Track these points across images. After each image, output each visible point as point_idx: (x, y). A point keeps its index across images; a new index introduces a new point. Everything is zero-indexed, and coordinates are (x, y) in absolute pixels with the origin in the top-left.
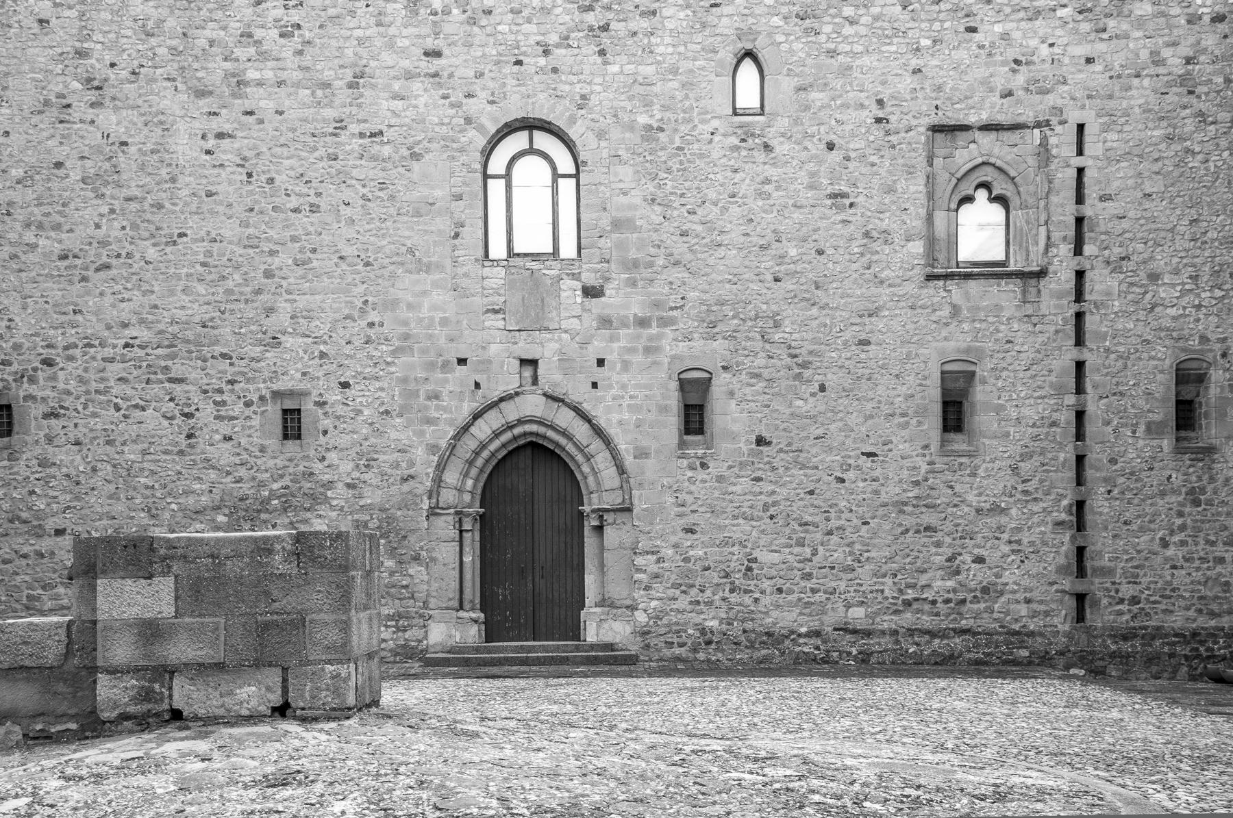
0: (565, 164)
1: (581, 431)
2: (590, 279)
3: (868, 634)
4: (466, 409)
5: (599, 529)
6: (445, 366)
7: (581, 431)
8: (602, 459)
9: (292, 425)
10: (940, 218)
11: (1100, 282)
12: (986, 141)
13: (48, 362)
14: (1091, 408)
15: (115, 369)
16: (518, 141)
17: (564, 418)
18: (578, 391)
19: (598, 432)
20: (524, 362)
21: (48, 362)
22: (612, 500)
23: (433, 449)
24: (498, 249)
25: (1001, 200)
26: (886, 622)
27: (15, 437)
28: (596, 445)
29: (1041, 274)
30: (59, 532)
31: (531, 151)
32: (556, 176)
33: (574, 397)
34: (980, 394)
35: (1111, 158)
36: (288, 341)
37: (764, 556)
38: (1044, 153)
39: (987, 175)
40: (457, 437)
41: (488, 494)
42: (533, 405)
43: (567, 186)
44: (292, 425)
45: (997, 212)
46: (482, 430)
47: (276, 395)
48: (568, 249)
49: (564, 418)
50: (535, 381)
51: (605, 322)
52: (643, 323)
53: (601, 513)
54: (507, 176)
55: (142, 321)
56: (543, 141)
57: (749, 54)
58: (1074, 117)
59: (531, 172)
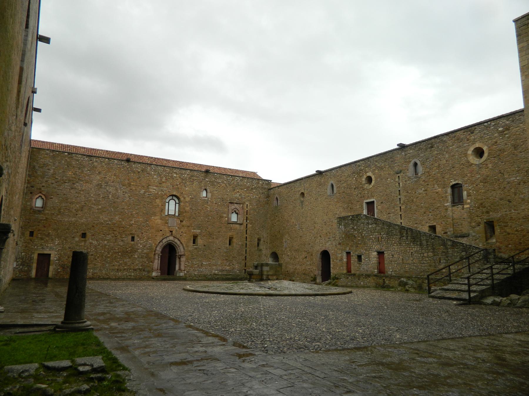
0: (177, 202)
1: (178, 243)
2: (181, 219)
3: (218, 275)
4: (161, 238)
5: (180, 258)
6: (158, 231)
7: (178, 243)
8: (181, 247)
9: (133, 239)
10: (230, 215)
11: (249, 226)
12: (236, 205)
13: (93, 226)
14: (248, 243)
15: (105, 228)
16: (171, 198)
17: (176, 240)
18: (178, 236)
19: (181, 243)
20: (171, 231)
21: (93, 226)
22: (183, 253)
23: (155, 244)
24: (166, 214)
25: (237, 213)
26: (220, 273)
27: (86, 239)
28: (180, 245)
29: (242, 224)
30: (92, 255)
31: (172, 199)
32: (176, 203)
33: (178, 237)
34: (234, 240)
35: (251, 209)
36: (134, 226)
37: (204, 263)
38: (243, 208)
39: (235, 210)
40: (159, 243)
41: (162, 252)
42: (171, 238)
43: (177, 205)
44: (133, 239)
45: (236, 215)
46: (164, 241)
47: (131, 234)
48: (177, 214)
49: (176, 240)
50: (172, 234)
51: (183, 226)
52: (188, 227)
53: (181, 255)
54: (169, 203)
55: (110, 221)
56: (174, 198)
57: (206, 190)
58: (247, 203)
59: (172, 203)
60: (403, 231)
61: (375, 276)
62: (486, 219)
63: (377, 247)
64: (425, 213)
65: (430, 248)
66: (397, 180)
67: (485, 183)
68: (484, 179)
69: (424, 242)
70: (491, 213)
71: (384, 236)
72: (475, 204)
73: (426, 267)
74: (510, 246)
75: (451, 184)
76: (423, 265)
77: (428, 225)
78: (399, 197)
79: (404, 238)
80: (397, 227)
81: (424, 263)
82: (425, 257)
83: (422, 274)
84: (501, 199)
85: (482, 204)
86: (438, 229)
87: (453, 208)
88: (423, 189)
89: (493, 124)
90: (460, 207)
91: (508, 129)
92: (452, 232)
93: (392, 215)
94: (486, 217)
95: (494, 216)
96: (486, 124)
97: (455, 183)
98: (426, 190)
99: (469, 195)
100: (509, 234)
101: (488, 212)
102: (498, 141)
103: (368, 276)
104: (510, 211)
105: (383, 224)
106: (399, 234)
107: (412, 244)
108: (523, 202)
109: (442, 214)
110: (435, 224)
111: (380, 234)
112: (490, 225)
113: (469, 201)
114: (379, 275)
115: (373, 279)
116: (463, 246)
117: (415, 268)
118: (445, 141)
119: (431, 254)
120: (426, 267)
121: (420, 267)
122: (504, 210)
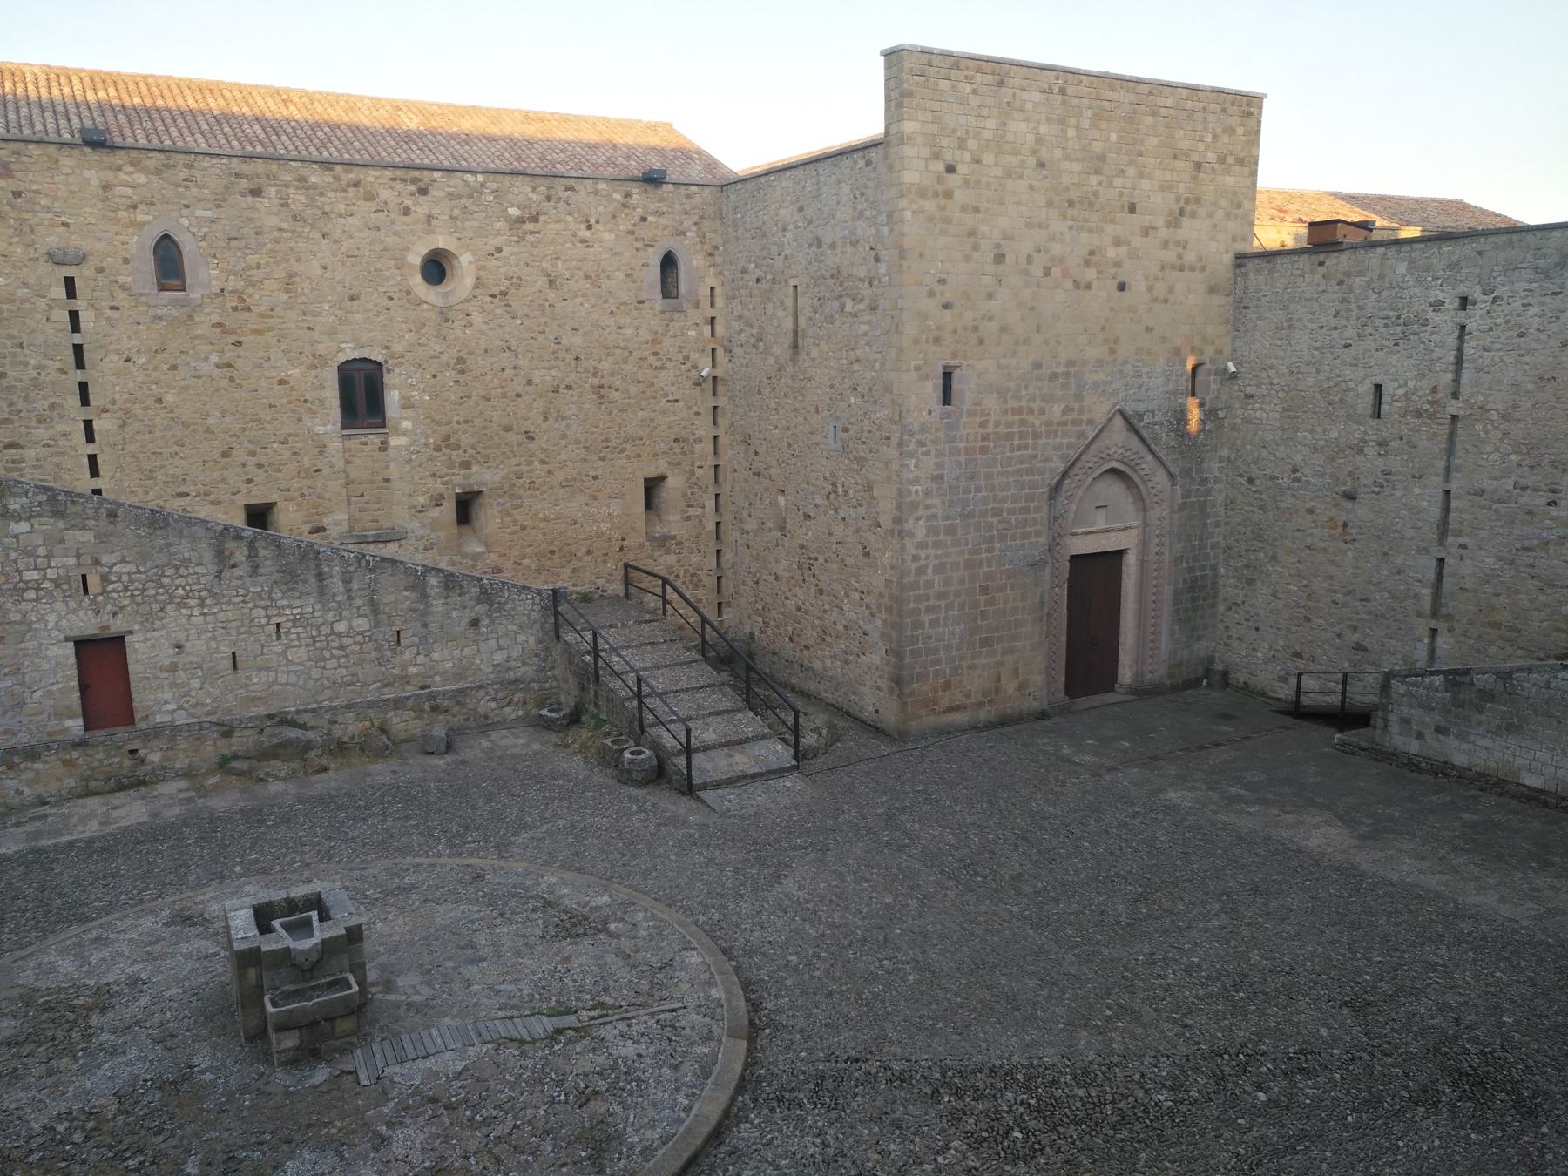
60: (230, 545)
61: (78, 744)
62: (461, 486)
63: (87, 623)
64: (225, 455)
65: (358, 602)
66: (61, 292)
67: (463, 372)
68: (461, 360)
69: (337, 586)
70: (475, 468)
71: (124, 568)
72: (428, 436)
73: (343, 671)
74: (525, 562)
75: (342, 358)
76: (331, 664)
77: (242, 500)
78: (79, 375)
79: (237, 572)
80: (201, 532)
81: (333, 657)
82: (340, 635)
83: (328, 693)
84: (508, 429)
85: (447, 438)
86: (290, 520)
87: (348, 443)
88: (214, 359)
89: (493, 186)
90: (374, 439)
91: (535, 219)
92: (345, 527)
93: (30, 454)
94: (459, 482)
95: (484, 476)
96: (469, 177)
97: (357, 355)
98: (229, 366)
99: (407, 405)
100: (523, 528)
101: (466, 465)
102: (505, 249)
103: (32, 754)
104: (530, 463)
105: (112, 515)
106: (208, 556)
107: (277, 594)
108: (563, 443)
109: (306, 462)
110: (274, 497)
111: (97, 562)
112: (465, 507)
113: (407, 424)
114: (100, 735)
115: (67, 763)
116: (481, 587)
117: (293, 679)
118: (315, 187)
119: (362, 624)
120: (343, 671)
121: (315, 674)
122: (517, 460)
